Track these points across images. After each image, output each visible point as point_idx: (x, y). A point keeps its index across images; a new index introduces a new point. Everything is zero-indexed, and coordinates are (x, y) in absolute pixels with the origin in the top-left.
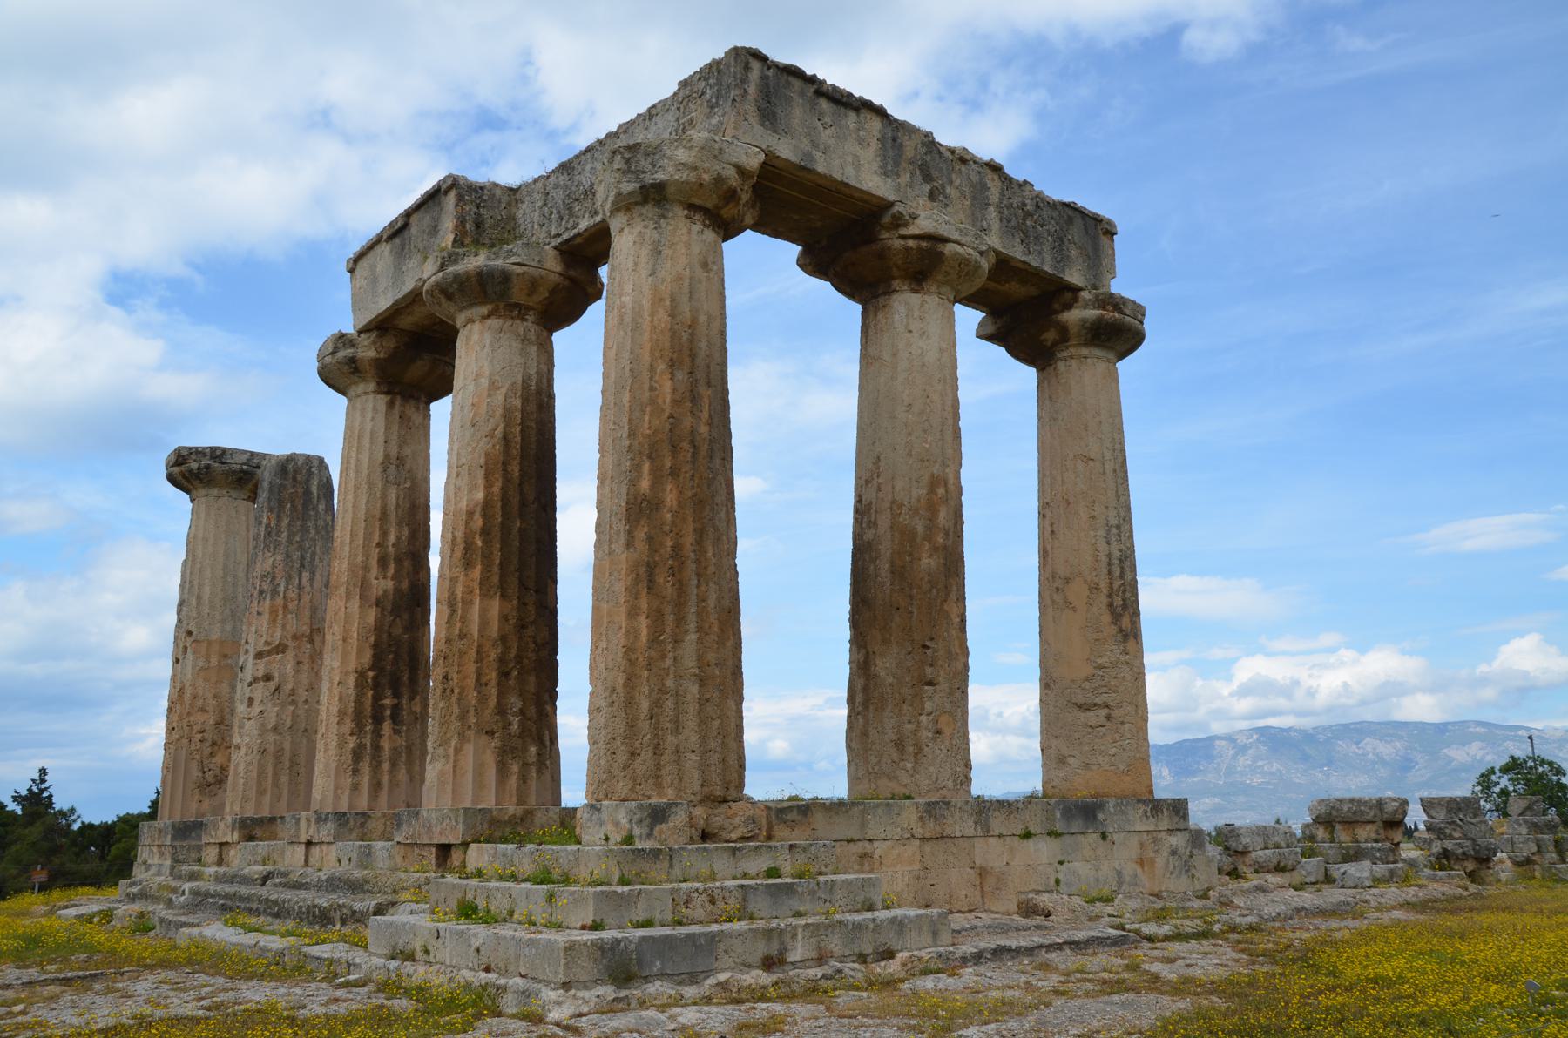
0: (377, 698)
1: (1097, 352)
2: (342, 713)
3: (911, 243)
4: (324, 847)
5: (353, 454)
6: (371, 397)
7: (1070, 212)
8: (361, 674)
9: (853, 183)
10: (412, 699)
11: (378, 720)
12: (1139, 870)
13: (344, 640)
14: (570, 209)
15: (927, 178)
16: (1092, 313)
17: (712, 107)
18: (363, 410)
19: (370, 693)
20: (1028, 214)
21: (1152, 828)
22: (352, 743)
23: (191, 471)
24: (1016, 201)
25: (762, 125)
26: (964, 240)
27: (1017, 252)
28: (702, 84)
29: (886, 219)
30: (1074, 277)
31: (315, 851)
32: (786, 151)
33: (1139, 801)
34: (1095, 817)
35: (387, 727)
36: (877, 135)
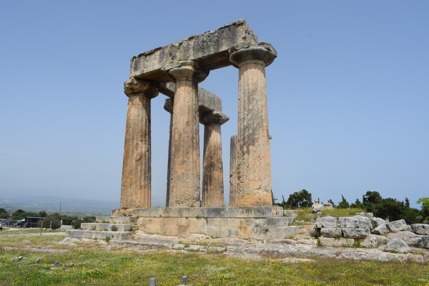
1: (242, 64)
7: (222, 30)
9: (151, 70)
10: (210, 186)
12: (239, 230)
15: (171, 54)
20: (205, 42)
21: (246, 217)
24: (201, 40)
25: (135, 71)
26: (173, 67)
27: (200, 55)
30: (224, 48)
32: (138, 73)
33: (240, 208)
34: (220, 213)
36: (159, 54)
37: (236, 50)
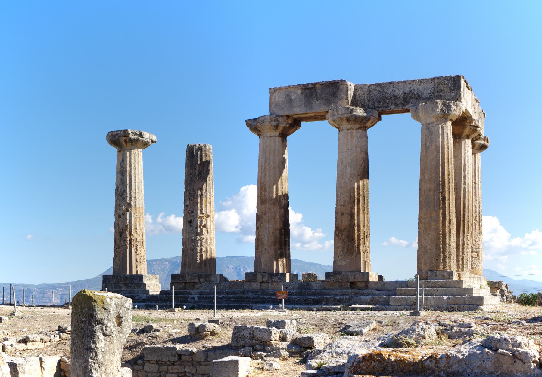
0: (285, 238)
2: (275, 243)
3: (472, 127)
4: (275, 284)
5: (272, 156)
6: (277, 138)
8: (280, 230)
11: (285, 245)
13: (274, 219)
14: (384, 100)
16: (482, 142)
17: (451, 90)
18: (275, 142)
19: (283, 237)
22: (279, 252)
23: (130, 140)
28: (447, 82)
29: (468, 121)
31: (263, 284)
35: (287, 246)
37: (488, 142)
